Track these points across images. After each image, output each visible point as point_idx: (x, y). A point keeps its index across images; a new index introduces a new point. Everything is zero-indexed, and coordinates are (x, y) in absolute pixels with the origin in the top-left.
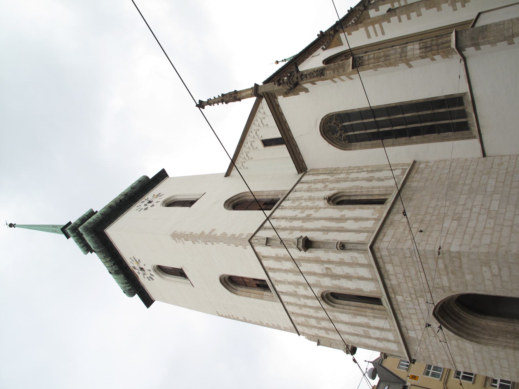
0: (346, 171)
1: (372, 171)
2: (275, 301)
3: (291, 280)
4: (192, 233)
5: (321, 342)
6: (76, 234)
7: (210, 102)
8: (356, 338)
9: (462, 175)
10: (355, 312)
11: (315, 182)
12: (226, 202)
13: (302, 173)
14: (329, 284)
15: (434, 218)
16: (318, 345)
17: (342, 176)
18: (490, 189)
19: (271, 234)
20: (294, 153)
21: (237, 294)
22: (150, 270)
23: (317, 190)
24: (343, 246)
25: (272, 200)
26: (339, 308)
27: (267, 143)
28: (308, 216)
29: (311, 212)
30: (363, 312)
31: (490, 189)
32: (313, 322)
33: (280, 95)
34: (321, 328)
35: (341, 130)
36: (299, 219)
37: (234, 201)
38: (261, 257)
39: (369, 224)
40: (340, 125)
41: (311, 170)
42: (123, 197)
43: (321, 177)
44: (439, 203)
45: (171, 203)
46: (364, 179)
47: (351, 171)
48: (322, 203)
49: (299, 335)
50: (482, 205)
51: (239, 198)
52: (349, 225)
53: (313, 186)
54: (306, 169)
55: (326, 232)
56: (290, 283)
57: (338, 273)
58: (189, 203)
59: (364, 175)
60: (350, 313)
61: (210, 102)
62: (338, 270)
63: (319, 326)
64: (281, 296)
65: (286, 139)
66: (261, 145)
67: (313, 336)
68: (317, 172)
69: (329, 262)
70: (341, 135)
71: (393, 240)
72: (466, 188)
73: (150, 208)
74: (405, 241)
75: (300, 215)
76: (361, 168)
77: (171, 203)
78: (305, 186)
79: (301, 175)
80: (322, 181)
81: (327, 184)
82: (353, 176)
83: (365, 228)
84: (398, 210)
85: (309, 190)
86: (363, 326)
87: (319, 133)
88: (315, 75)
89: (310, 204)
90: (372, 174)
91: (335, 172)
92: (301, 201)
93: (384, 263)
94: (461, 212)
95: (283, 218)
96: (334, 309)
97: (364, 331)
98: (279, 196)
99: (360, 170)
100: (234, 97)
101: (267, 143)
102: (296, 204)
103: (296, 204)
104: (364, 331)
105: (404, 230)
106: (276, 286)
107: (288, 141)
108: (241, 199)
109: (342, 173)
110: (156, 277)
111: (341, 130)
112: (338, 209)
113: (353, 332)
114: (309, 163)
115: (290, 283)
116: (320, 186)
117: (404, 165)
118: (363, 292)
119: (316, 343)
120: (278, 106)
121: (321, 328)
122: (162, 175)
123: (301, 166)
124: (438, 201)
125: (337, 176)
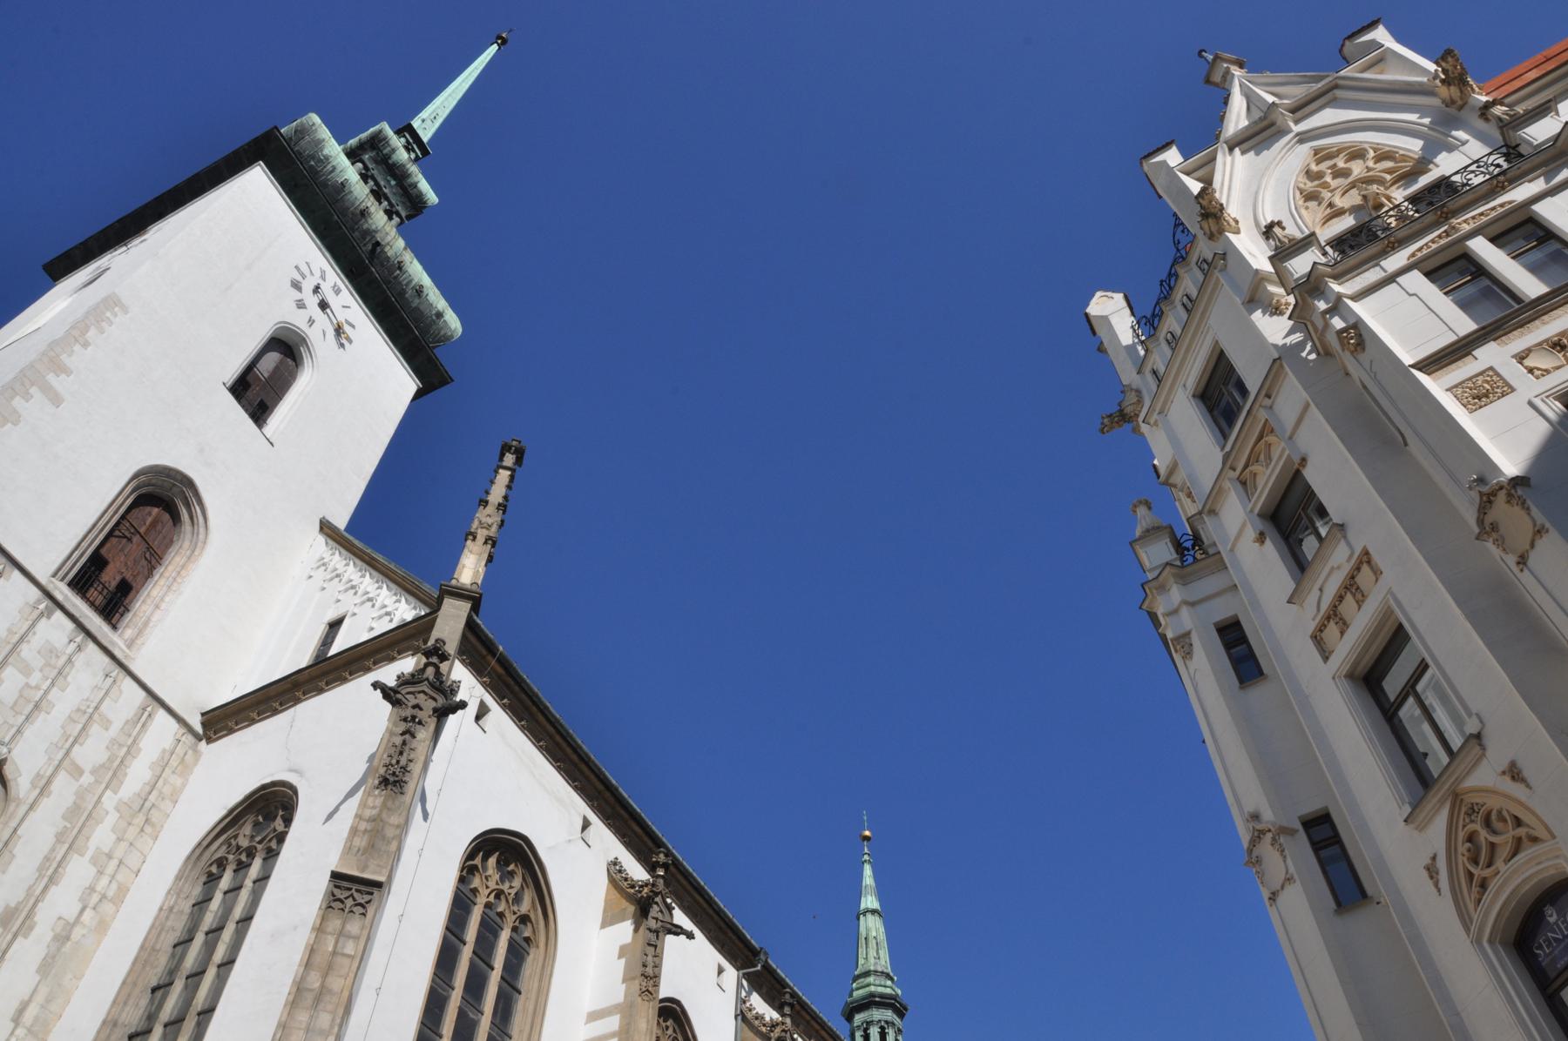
0: (118, 854)
4: (86, 345)
13: (204, 724)
17: (102, 836)
45: (286, 349)
54: (209, 740)
59: (62, 902)
73: (297, 295)
77: (286, 349)
79: (196, 723)
80: (113, 772)
82: (79, 871)
85: (89, 716)
87: (268, 780)
99: (95, 898)
109: (119, 840)
116: (92, 752)
125: (111, 818)
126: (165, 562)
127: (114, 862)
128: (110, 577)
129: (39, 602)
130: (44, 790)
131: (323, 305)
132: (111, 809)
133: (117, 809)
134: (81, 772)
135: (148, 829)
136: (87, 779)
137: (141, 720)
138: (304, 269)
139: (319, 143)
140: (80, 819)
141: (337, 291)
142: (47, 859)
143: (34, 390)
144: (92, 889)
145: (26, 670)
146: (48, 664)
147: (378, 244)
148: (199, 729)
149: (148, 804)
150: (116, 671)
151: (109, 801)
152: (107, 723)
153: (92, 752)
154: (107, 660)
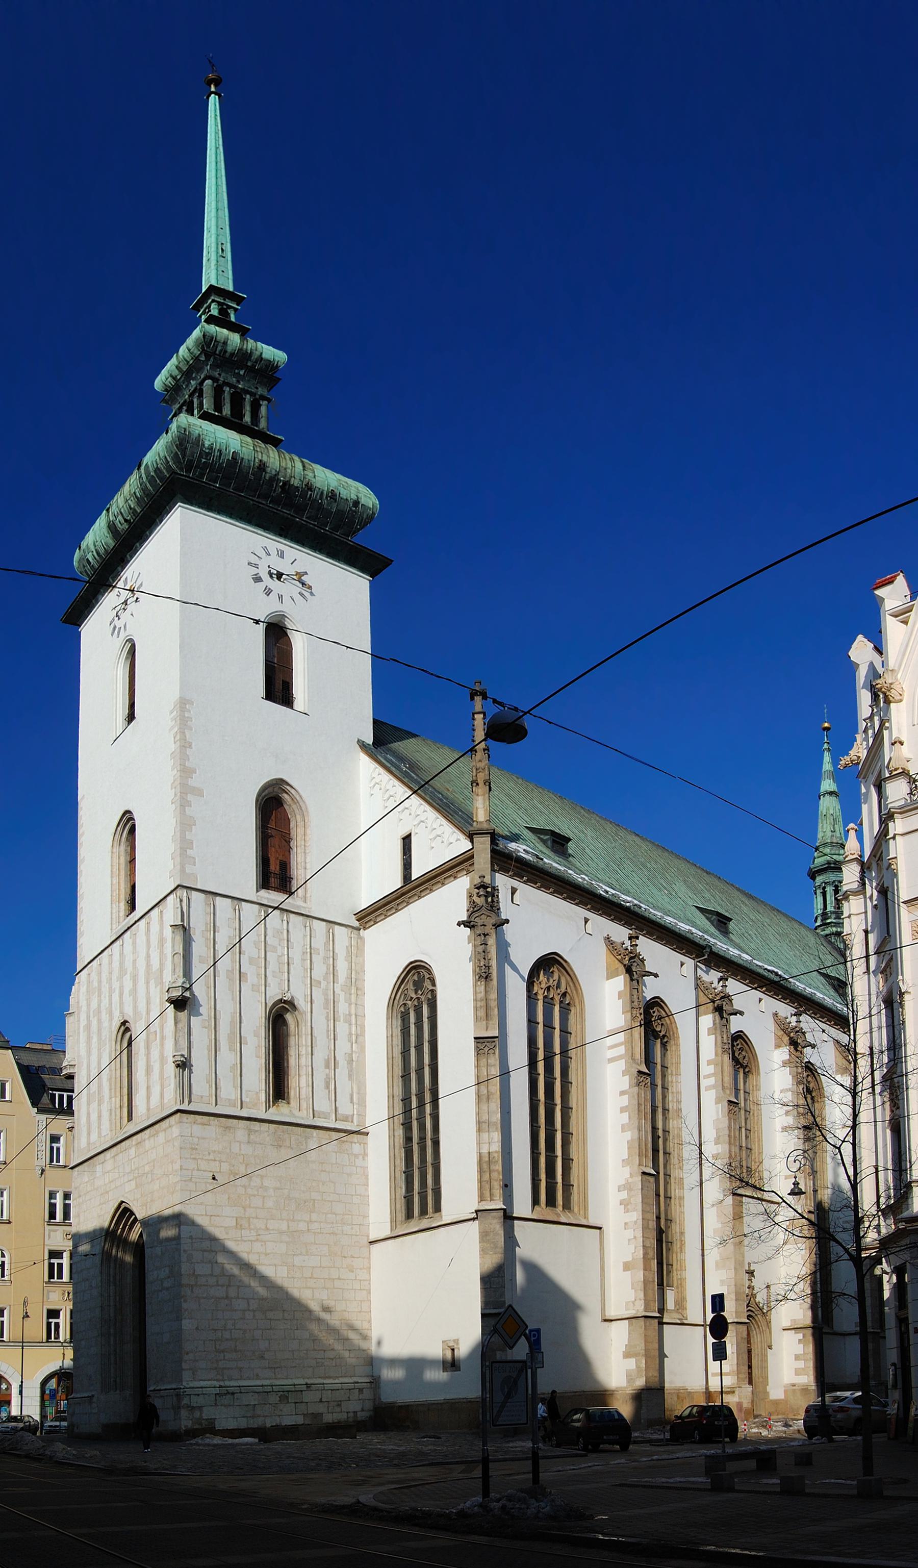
0: (353, 1012)
1: (350, 1061)
9: (329, 1216)
15: (241, 1190)
17: (342, 1007)
18: (297, 1261)
31: (297, 1261)
39: (228, 1091)
41: (362, 939)
44: (271, 1192)
47: (354, 1022)
50: (266, 1254)
52: (227, 1057)
54: (365, 929)
59: (343, 1046)
68: (356, 952)
71: (196, 1140)
72: (302, 1226)
74: (195, 1159)
76: (360, 1039)
78: (319, 941)
84: (257, 1131)
93: (165, 1130)
94: (252, 1227)
99: (354, 1037)
105: (214, 1152)
109: (350, 1004)
116: (319, 970)
117: (362, 1116)
124: (276, 1189)
126: (293, 833)
127: (354, 1016)
128: (274, 867)
129: (260, 912)
132: (340, 992)
133: (342, 990)
134: (320, 983)
135: (359, 993)
136: (323, 984)
137: (331, 939)
142: (328, 1031)
144: (350, 1034)
146: (280, 940)
149: (353, 980)
150: (308, 921)
153: (319, 970)
154: (301, 918)
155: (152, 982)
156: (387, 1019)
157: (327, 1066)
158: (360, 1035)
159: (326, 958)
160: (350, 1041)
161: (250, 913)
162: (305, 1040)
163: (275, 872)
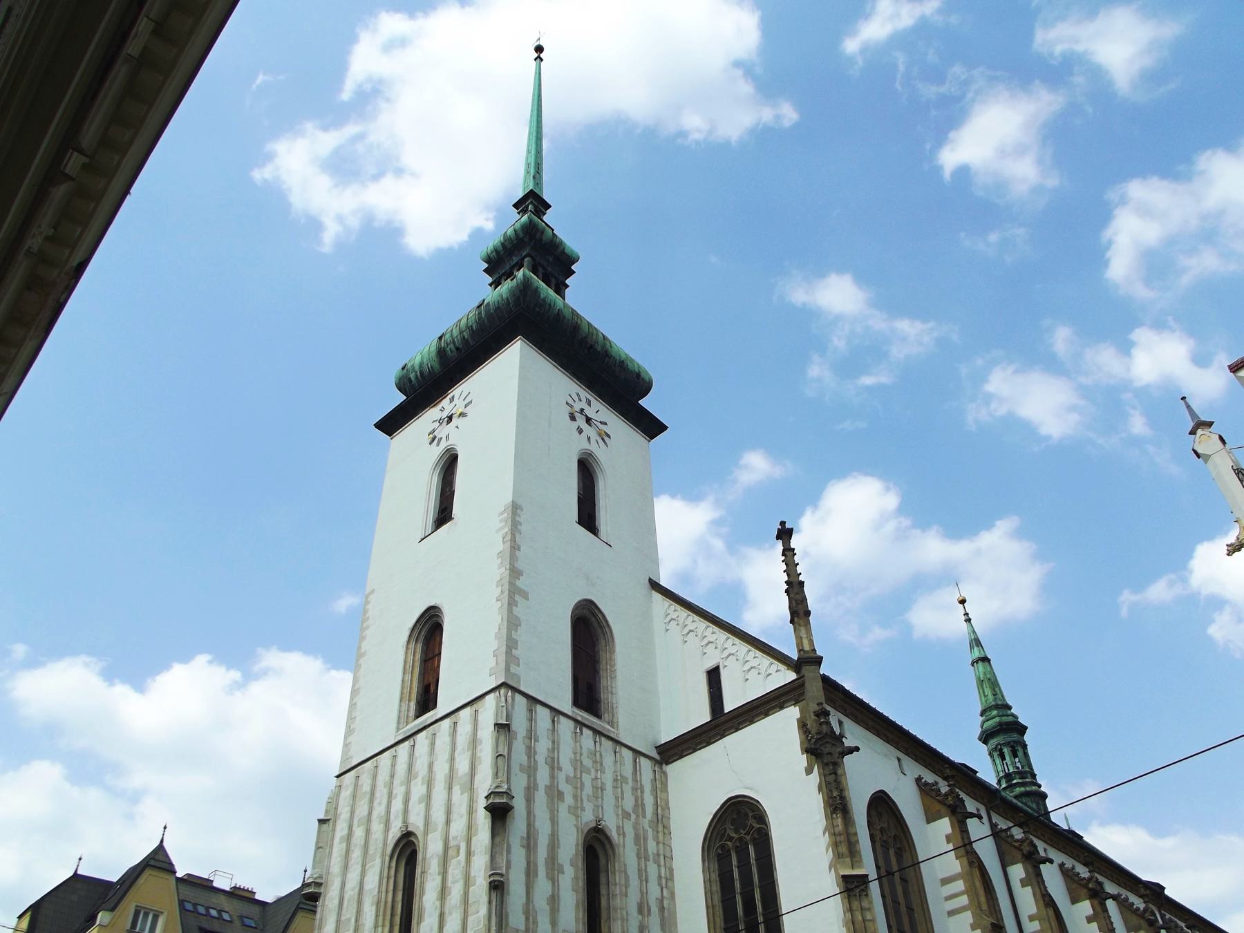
0: (661, 852)
1: (662, 909)
2: (398, 729)
3: (435, 768)
5: (325, 826)
6: (521, 235)
7: (788, 552)
8: (336, 902)
10: (383, 904)
11: (638, 789)
12: (591, 602)
14: (431, 849)
16: (320, 821)
17: (652, 846)
19: (520, 725)
20: (692, 738)
21: (408, 642)
22: (447, 438)
23: (619, 799)
24: (497, 887)
25: (598, 701)
26: (389, 868)
27: (714, 676)
28: (560, 795)
29: (569, 799)
30: (384, 920)
32: (362, 810)
33: (801, 711)
34: (350, 827)
35: (740, 839)
36: (552, 777)
37: (595, 615)
38: (475, 706)
40: (748, 838)
41: (665, 774)
42: (599, 348)
43: (649, 800)
45: (587, 470)
46: (644, 894)
48: (588, 817)
49: (338, 777)
51: (601, 627)
52: (543, 886)
53: (628, 789)
54: (667, 763)
55: (525, 842)
56: (431, 765)
57: (450, 870)
58: (588, 518)
59: (654, 891)
60: (380, 892)
61: (788, 552)
62: (455, 871)
63: (355, 822)
64: (406, 743)
65: (723, 722)
66: (710, 664)
67: (336, 809)
68: (660, 786)
69: (469, 854)
70: (730, 839)
73: (574, 425)
75: (561, 777)
76: (670, 884)
77: (587, 470)
78: (628, 770)
79: (655, 754)
80: (639, 805)
81: (633, 817)
82: (652, 869)
83: (535, 922)
85: (618, 781)
86: (357, 921)
87: (733, 795)
88: (835, 794)
89: (588, 790)
90: (655, 910)
91: (660, 828)
92: (593, 771)
95: (553, 742)
96: (387, 859)
97: (349, 920)
98: (606, 716)
99: (664, 881)
100: (799, 611)
101: (714, 676)
102: (587, 762)
103: (587, 762)
104: (349, 920)
106: (424, 733)
107: (716, 726)
108: (599, 631)
109: (658, 843)
110: (436, 452)
111: (740, 839)
112: (576, 855)
113: (347, 897)
114: (676, 769)
115: (431, 765)
116: (629, 803)
118: (419, 923)
119: (322, 817)
120: (781, 707)
121: (350, 827)
122: (651, 427)
123: (672, 751)
130: (624, 836)
131: (588, 420)
134: (629, 815)
136: (633, 817)
138: (571, 402)
139: (536, 291)
140: (639, 839)
141: (589, 403)
143: (517, 598)
145: (589, 772)
147: (591, 347)
148: (657, 757)
151: (645, 823)
152: (624, 780)
155: (456, 790)
156: (703, 861)
157: (640, 911)
158: (667, 881)
159: (634, 789)
160: (660, 884)
161: (565, 726)
162: (618, 878)
163: (588, 690)
